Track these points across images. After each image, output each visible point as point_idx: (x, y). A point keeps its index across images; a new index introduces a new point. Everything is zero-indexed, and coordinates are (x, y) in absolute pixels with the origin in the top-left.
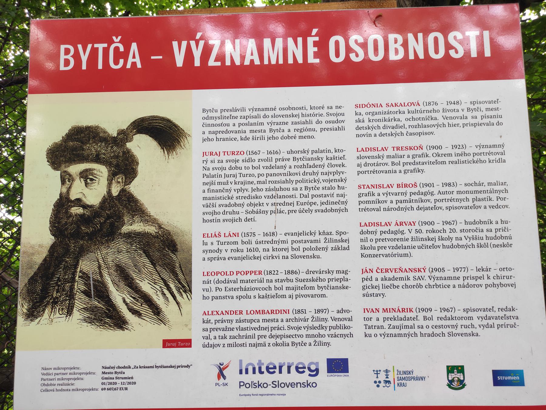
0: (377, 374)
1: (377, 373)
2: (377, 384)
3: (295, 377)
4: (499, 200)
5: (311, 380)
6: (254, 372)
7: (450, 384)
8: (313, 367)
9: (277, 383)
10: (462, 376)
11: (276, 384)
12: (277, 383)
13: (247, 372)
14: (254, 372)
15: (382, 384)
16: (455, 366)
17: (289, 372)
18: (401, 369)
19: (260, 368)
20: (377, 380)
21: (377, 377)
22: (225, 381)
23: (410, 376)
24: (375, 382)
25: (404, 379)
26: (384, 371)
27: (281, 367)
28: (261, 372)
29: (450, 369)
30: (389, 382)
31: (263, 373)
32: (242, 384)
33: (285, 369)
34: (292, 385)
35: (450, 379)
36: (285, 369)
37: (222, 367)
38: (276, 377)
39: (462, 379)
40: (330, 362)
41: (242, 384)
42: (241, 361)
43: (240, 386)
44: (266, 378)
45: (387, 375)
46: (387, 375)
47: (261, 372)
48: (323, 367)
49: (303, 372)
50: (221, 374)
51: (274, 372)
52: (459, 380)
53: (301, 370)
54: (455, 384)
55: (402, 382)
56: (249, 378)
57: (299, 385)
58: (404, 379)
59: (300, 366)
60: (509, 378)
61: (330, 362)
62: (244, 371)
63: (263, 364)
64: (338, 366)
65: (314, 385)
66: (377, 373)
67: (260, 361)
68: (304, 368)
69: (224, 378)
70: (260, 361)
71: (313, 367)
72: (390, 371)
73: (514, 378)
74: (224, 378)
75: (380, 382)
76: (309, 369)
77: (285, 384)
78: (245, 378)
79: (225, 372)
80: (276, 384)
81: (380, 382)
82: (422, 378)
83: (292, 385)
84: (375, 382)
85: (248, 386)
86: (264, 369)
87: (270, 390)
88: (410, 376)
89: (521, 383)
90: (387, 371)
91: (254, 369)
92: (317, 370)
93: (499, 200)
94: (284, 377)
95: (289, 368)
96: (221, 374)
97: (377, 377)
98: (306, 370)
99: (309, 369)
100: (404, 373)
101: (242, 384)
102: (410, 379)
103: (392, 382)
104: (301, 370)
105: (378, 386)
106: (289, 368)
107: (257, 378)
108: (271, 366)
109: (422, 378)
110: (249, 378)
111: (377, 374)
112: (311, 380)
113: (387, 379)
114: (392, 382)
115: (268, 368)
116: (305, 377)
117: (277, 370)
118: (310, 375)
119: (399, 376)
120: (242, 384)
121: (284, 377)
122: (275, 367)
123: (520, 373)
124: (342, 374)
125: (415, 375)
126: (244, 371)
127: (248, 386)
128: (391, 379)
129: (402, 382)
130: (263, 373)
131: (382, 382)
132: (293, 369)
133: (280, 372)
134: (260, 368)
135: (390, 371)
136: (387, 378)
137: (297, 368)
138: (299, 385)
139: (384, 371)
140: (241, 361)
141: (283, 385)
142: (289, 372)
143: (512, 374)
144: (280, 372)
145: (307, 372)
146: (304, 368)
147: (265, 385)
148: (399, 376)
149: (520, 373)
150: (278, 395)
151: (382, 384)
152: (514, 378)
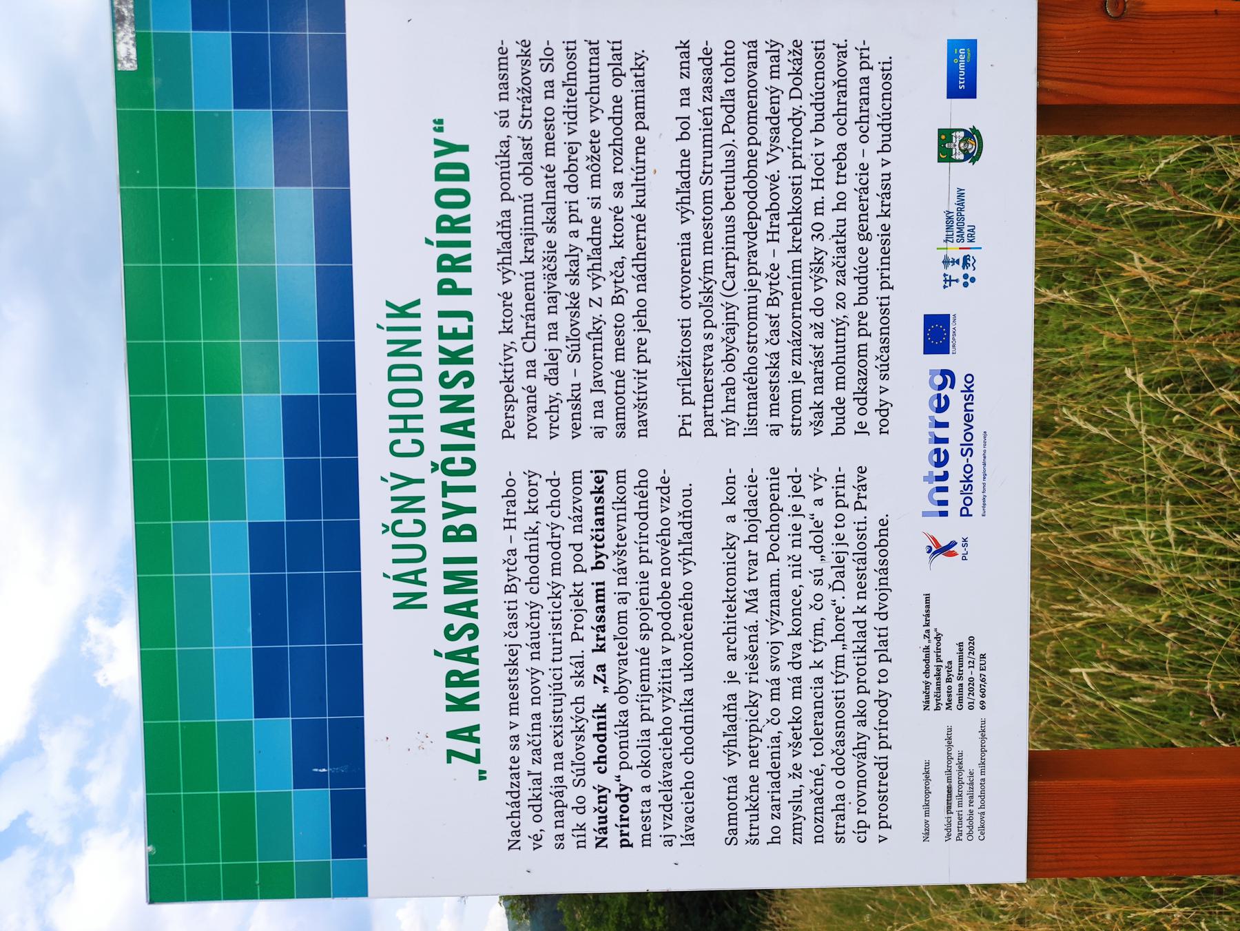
0: (950, 281)
1: (949, 281)
2: (968, 280)
3: (954, 415)
4: (777, 555)
5: (960, 384)
6: (945, 489)
7: (972, 157)
8: (939, 380)
9: (965, 448)
10: (958, 134)
11: (967, 450)
12: (965, 448)
13: (945, 503)
14: (945, 489)
15: (969, 271)
16: (939, 146)
17: (946, 425)
18: (943, 234)
19: (938, 479)
20: (962, 280)
21: (957, 281)
22: (960, 542)
23: (955, 217)
24: (966, 285)
25: (960, 230)
26: (946, 267)
27: (938, 440)
28: (945, 476)
29: (945, 155)
30: (966, 258)
31: (946, 474)
32: (964, 512)
33: (941, 433)
34: (968, 419)
35: (962, 157)
36: (941, 433)
37: (934, 549)
38: (953, 448)
39: (962, 134)
40: (929, 349)
41: (965, 513)
42: (925, 514)
43: (968, 515)
44: (955, 466)
45: (953, 262)
46: (953, 262)
47: (945, 476)
48: (939, 361)
49: (946, 398)
50: (947, 550)
51: (946, 452)
52: (964, 140)
53: (943, 403)
54: (971, 148)
55: (966, 233)
56: (954, 498)
57: (969, 407)
58: (960, 230)
59: (935, 403)
60: (962, 67)
61: (929, 349)
62: (943, 508)
63: (931, 473)
64: (937, 334)
65: (969, 379)
66: (949, 281)
67: (925, 479)
68: (939, 396)
69: (953, 544)
70: (925, 479)
71: (939, 380)
72: (946, 256)
73: (962, 58)
74: (953, 544)
75: (966, 276)
76: (941, 387)
77: (967, 432)
78: (954, 507)
79: (943, 544)
80: (967, 450)
81: (966, 276)
82: (961, 194)
83: (968, 419)
84: (966, 285)
85: (968, 501)
86: (939, 472)
87: (976, 461)
88: (955, 217)
89: (972, 45)
90: (946, 262)
91: (939, 489)
92: (944, 373)
93: (777, 555)
94: (955, 433)
95: (939, 425)
96: (947, 550)
97: (957, 281)
98: (943, 393)
99: (941, 387)
100: (949, 228)
101: (964, 512)
102: (961, 218)
103: (966, 252)
104: (943, 403)
105: (973, 280)
106: (939, 425)
107: (954, 483)
108: (935, 458)
109: (961, 194)
110: (954, 498)
111: (950, 281)
112: (960, 384)
113: (961, 262)
114: (966, 252)
115: (939, 464)
116: (956, 396)
117: (942, 447)
118: (952, 386)
119: (955, 238)
120: (965, 513)
121: (955, 433)
122: (937, 451)
123: (953, 45)
124: (951, 327)
125: (954, 208)
126: (943, 508)
127: (968, 501)
128: (960, 255)
129: (966, 233)
130: (946, 474)
131: (966, 271)
132: (941, 418)
133: (946, 441)
134: (938, 479)
135: (946, 256)
136: (958, 262)
137: (940, 410)
138: (969, 407)
139: (946, 267)
140: (925, 514)
141: (969, 437)
142: (946, 425)
143: (956, 61)
144: (946, 441)
145: (946, 391)
146: (939, 396)
147: (968, 469)
148: (955, 238)
149: (953, 45)
150: (927, 814)
151: (969, 271)
152: (962, 58)
